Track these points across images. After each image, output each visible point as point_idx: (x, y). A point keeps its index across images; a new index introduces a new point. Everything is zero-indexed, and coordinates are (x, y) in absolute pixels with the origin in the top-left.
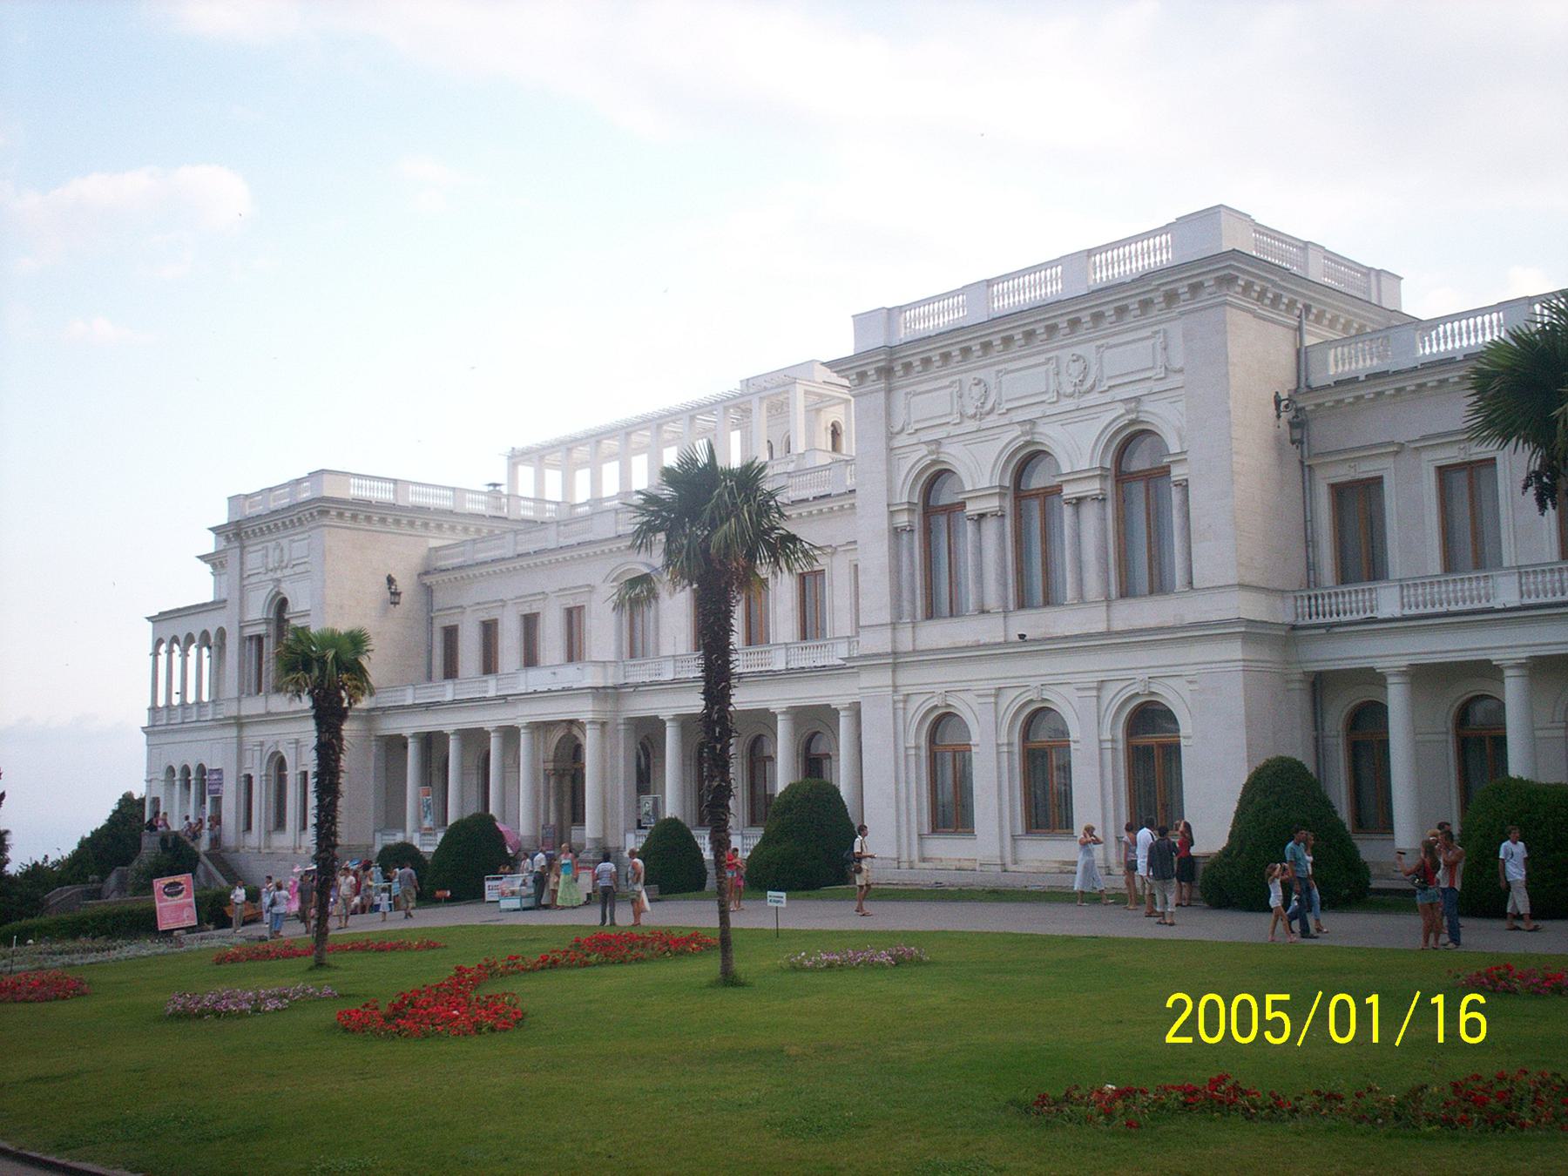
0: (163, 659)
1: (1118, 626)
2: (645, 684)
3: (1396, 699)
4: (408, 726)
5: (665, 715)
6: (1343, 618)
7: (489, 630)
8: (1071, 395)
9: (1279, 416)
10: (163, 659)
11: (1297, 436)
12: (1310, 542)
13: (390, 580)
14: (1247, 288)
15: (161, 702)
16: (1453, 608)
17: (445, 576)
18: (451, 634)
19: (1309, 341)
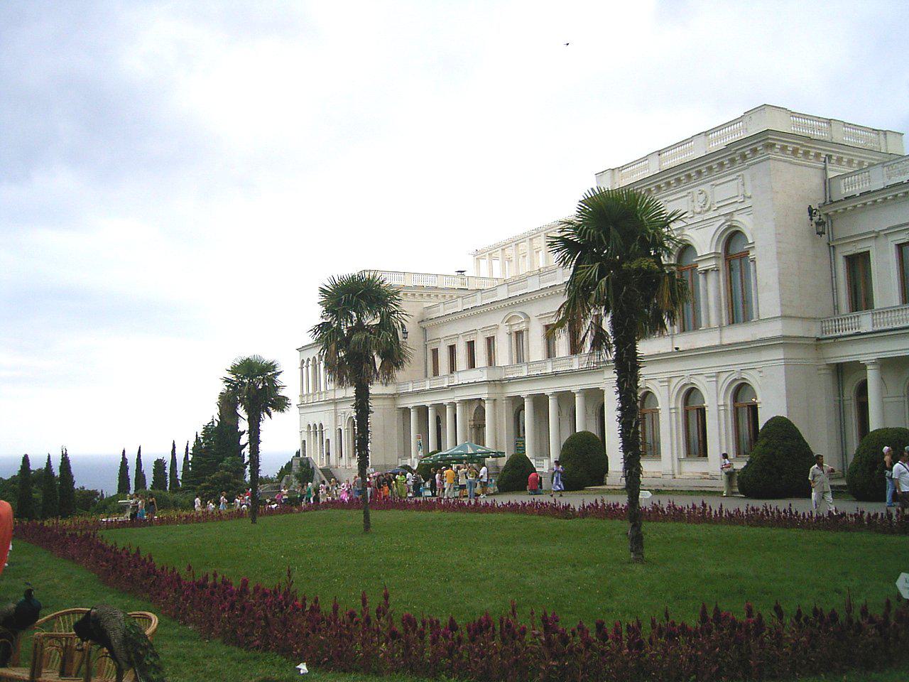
0: (304, 369)
1: (726, 341)
2: (514, 378)
3: (872, 377)
4: (410, 403)
5: (524, 395)
6: (845, 333)
7: (452, 349)
8: (700, 213)
9: (811, 219)
10: (304, 369)
11: (820, 229)
12: (834, 289)
14: (783, 149)
15: (305, 392)
16: (895, 326)
17: (431, 323)
18: (435, 352)
19: (831, 175)
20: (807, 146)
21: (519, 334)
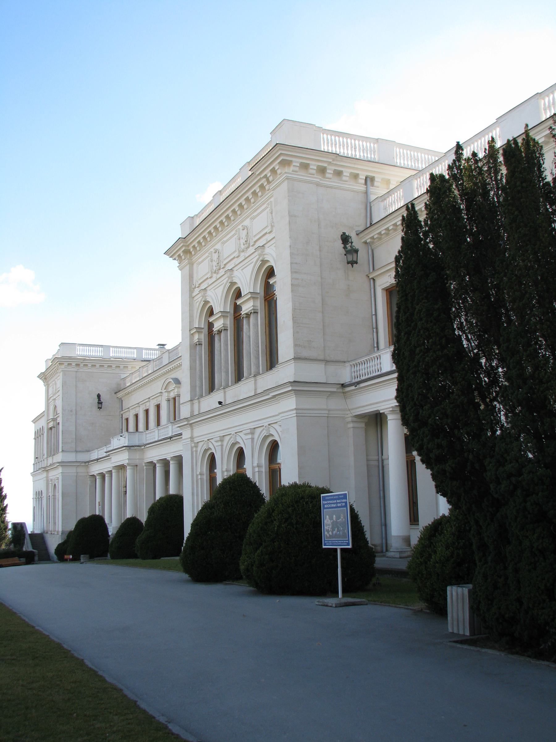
11: (350, 258)
13: (99, 396)
20: (353, 168)
21: (174, 399)
